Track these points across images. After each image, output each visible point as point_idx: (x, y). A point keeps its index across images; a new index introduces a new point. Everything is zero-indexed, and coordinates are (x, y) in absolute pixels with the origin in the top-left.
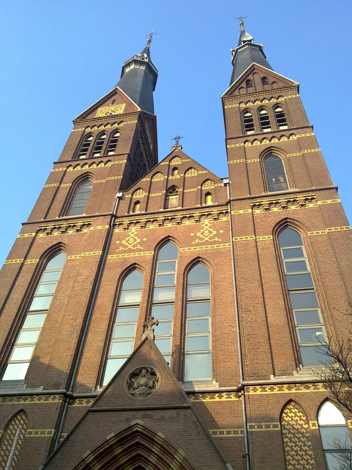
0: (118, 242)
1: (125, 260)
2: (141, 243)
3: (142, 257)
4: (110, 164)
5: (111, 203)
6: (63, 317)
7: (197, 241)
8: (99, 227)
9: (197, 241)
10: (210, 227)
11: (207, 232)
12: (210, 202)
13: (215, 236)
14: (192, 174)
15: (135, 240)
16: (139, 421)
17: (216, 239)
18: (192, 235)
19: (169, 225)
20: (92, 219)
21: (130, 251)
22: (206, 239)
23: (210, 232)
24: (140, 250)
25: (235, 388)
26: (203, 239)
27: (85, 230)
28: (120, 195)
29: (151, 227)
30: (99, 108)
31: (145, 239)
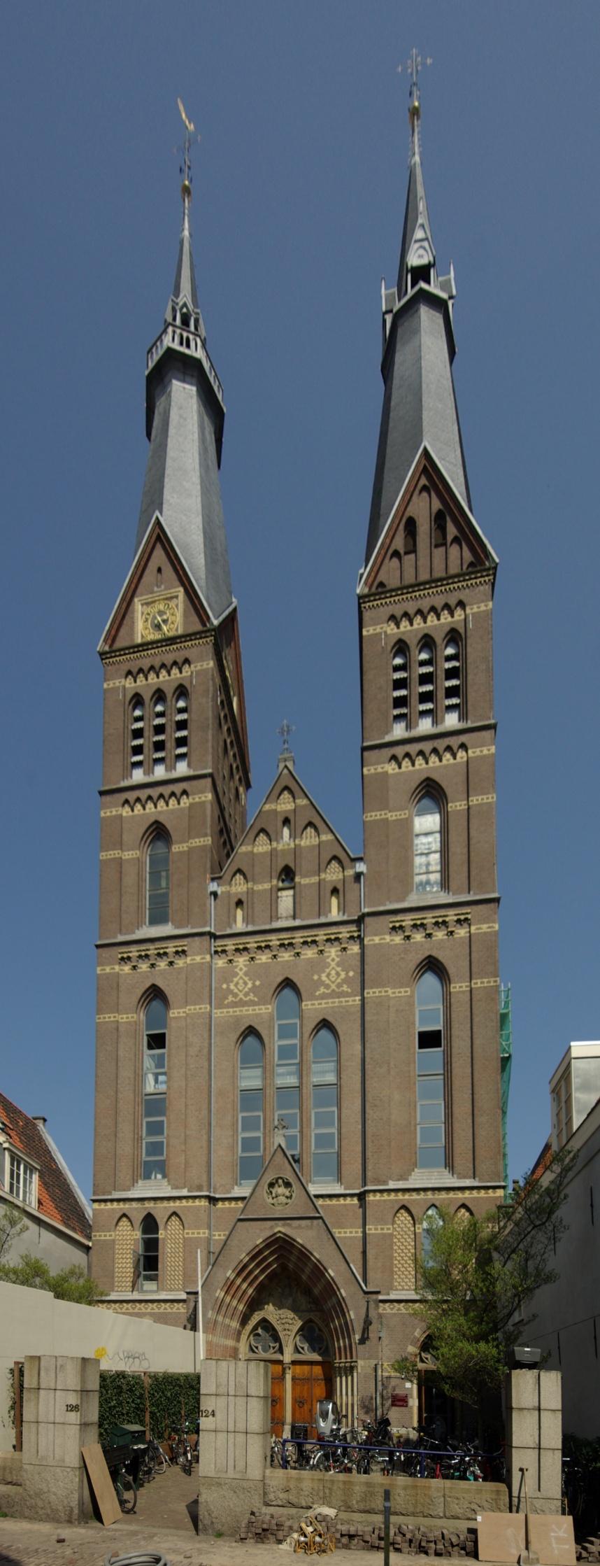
0: (224, 986)
1: (238, 1019)
2: (254, 989)
3: (257, 1015)
4: (185, 801)
5: (205, 905)
6: (186, 1106)
7: (322, 990)
8: (198, 959)
9: (322, 990)
10: (338, 965)
11: (333, 972)
12: (334, 914)
13: (344, 981)
14: (309, 839)
15: (245, 983)
16: (280, 1228)
17: (345, 988)
18: (316, 977)
19: (286, 956)
20: (185, 942)
21: (242, 1003)
22: (333, 987)
23: (338, 974)
24: (252, 1003)
25: (357, 1191)
26: (327, 987)
27: (180, 962)
28: (213, 887)
29: (264, 958)
30: (136, 600)
31: (258, 983)
